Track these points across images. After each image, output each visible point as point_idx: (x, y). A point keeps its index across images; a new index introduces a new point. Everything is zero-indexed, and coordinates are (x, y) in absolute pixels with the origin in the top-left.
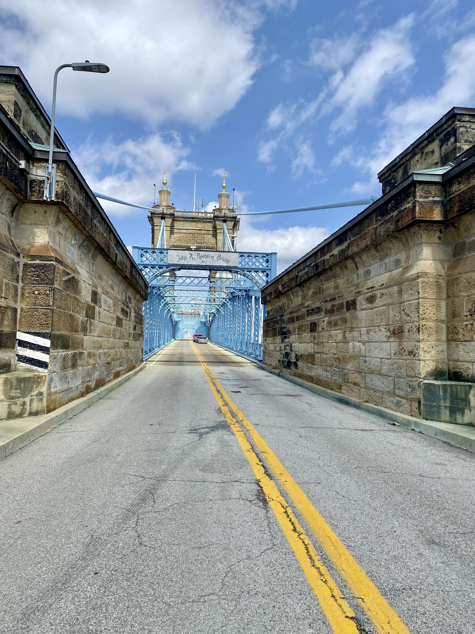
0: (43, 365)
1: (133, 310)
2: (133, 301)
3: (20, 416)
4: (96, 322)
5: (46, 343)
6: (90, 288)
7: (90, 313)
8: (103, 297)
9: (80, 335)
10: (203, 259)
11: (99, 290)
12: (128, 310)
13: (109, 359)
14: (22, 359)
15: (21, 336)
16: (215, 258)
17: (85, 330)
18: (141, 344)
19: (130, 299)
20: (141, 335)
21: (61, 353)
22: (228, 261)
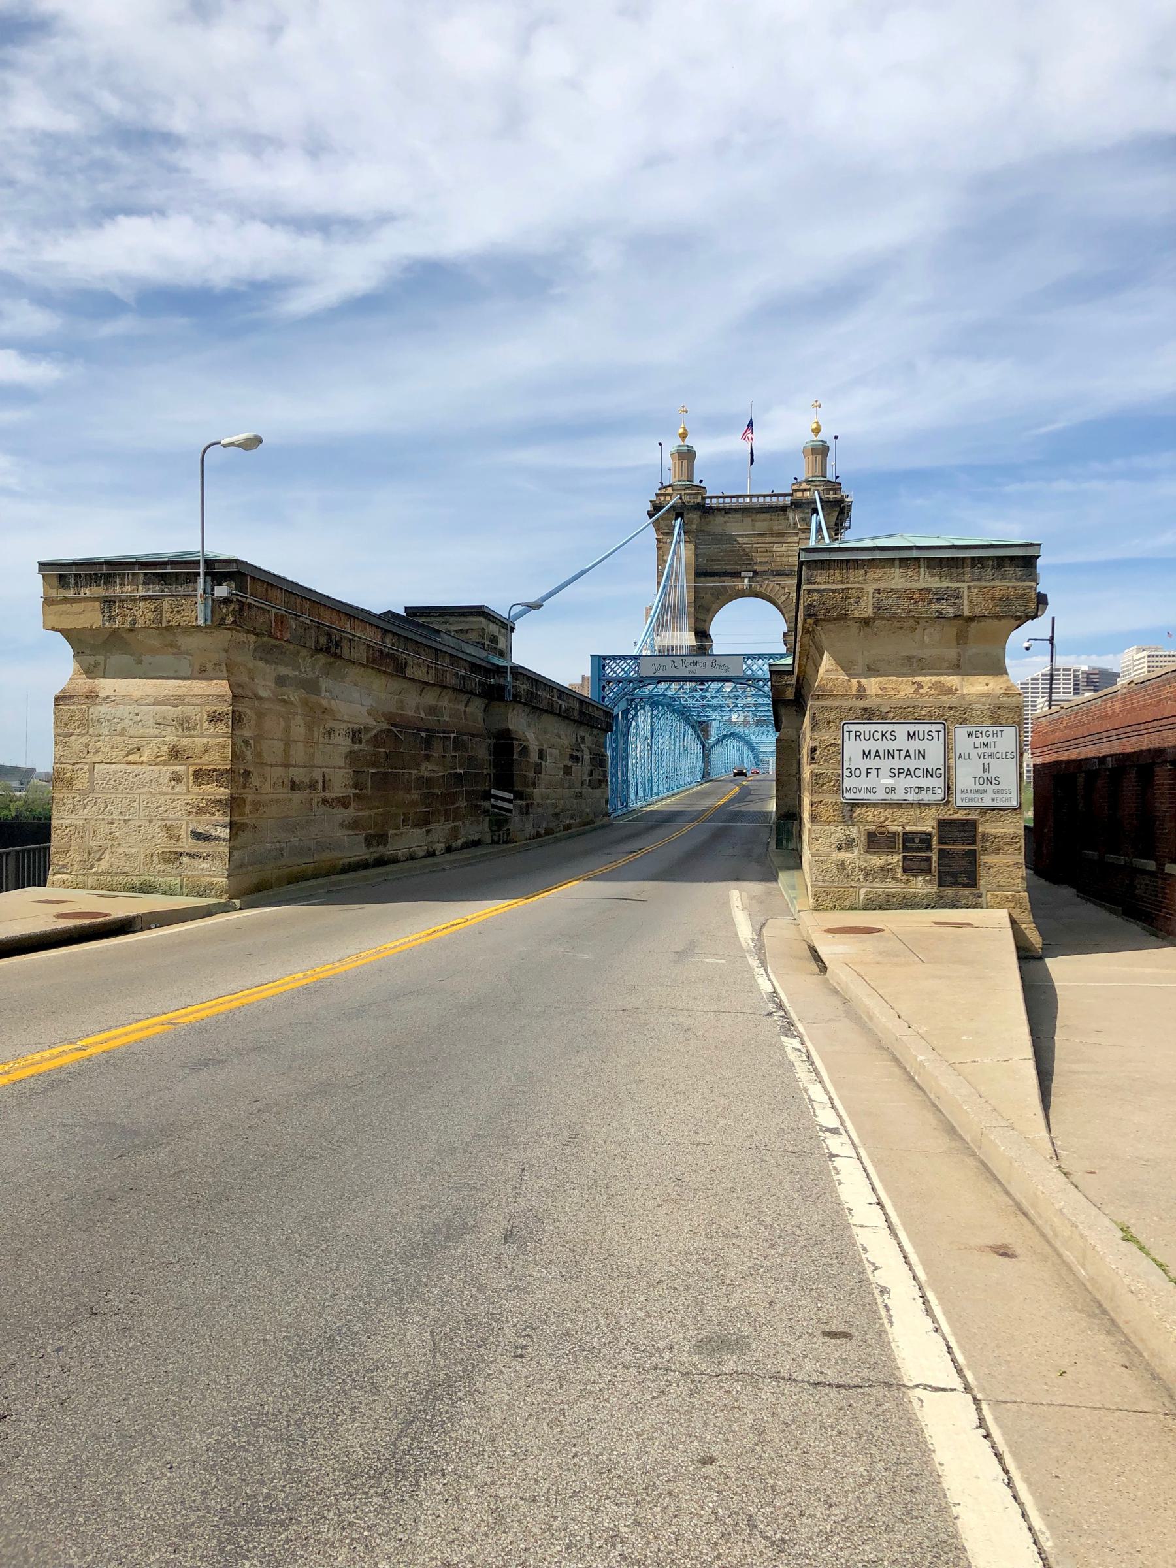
0: (510, 811)
1: (586, 752)
2: (589, 739)
3: (498, 843)
4: (542, 776)
5: (511, 796)
6: (537, 748)
7: (538, 769)
9: (530, 790)
10: (691, 668)
11: (545, 747)
12: (579, 754)
13: (557, 810)
14: (494, 806)
15: (494, 792)
16: (708, 665)
17: (534, 785)
18: (603, 793)
19: (583, 738)
20: (603, 781)
21: (519, 802)
22: (727, 669)
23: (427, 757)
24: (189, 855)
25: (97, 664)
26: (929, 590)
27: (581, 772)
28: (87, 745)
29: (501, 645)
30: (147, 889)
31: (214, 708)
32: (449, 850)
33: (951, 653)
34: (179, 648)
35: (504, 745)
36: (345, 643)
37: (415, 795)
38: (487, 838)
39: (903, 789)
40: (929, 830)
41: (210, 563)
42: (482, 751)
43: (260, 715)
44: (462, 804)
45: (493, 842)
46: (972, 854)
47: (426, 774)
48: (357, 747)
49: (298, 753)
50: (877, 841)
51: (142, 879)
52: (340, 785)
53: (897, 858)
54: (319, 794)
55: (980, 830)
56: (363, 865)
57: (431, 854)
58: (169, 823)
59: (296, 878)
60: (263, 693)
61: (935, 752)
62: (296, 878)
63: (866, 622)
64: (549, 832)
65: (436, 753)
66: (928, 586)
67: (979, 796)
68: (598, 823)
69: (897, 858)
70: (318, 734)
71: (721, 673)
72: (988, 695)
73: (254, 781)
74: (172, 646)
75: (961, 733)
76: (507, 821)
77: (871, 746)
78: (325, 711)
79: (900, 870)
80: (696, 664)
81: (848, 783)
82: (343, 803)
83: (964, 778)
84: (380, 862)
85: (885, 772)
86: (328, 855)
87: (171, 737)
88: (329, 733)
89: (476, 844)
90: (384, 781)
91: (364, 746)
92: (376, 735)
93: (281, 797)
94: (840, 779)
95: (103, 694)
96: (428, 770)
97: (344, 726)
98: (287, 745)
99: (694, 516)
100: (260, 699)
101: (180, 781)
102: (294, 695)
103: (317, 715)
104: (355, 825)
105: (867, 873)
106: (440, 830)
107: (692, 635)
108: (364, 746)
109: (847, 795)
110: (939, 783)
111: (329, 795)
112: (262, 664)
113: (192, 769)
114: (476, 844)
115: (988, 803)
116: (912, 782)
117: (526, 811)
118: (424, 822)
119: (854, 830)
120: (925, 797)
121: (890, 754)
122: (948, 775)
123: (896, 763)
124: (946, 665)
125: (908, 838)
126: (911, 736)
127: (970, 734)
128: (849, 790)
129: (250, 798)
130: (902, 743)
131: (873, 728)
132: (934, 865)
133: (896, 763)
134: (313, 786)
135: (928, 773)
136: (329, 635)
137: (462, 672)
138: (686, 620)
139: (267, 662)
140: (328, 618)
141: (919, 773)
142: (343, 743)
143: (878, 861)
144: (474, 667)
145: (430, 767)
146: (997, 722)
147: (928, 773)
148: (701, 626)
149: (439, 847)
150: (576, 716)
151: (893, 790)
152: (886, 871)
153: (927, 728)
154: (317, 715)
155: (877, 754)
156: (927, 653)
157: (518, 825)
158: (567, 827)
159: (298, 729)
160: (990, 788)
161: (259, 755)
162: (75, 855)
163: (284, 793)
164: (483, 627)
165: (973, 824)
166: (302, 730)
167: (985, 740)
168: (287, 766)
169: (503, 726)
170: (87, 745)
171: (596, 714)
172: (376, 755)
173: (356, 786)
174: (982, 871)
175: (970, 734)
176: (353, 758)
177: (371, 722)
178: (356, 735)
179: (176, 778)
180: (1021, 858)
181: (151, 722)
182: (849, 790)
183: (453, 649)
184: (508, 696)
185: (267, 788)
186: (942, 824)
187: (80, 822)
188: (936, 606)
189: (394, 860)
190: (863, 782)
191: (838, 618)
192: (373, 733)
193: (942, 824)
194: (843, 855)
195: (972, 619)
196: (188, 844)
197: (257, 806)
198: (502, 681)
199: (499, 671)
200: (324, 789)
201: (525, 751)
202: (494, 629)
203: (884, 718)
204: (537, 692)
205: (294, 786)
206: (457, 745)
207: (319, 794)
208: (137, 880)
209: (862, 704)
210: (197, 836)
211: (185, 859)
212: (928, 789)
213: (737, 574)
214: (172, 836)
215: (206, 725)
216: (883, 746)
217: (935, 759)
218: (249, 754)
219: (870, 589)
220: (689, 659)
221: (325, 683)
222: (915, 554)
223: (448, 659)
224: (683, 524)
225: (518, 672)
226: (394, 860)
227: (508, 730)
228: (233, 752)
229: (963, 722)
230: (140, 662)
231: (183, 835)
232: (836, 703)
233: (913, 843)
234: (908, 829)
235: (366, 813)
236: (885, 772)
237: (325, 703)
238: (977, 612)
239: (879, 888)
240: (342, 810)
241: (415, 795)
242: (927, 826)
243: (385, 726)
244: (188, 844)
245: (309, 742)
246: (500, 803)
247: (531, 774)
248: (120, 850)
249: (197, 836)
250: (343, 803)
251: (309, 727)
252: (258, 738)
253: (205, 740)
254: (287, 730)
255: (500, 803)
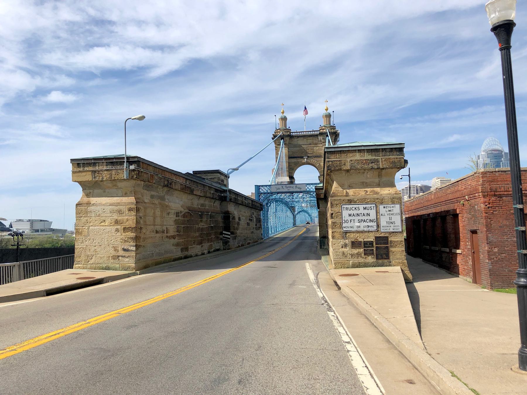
0: (229, 238)
1: (254, 218)
5: (229, 233)
7: (238, 224)
8: (242, 218)
9: (236, 231)
15: (224, 232)
16: (294, 187)
17: (237, 229)
20: (260, 227)
23: (201, 221)
24: (122, 256)
25: (90, 193)
26: (368, 160)
27: (253, 224)
28: (87, 220)
29: (225, 183)
30: (107, 268)
31: (129, 207)
32: (209, 252)
33: (377, 180)
34: (118, 186)
35: (227, 216)
36: (173, 184)
37: (197, 234)
38: (222, 248)
39: (363, 226)
40: (372, 240)
41: (128, 158)
42: (220, 218)
43: (145, 208)
44: (213, 236)
45: (224, 249)
46: (387, 248)
47: (201, 227)
48: (177, 218)
49: (158, 221)
50: (355, 244)
51: (106, 265)
52: (172, 231)
53: (362, 250)
54: (165, 235)
55: (390, 239)
56: (180, 258)
57: (203, 254)
58: (115, 246)
59: (157, 264)
60: (146, 201)
61: (373, 213)
62: (157, 264)
63: (348, 171)
64: (242, 245)
65: (204, 219)
66: (368, 158)
67: (388, 228)
68: (259, 242)
69: (362, 250)
70: (165, 214)
71: (299, 190)
72: (390, 194)
73: (144, 231)
74: (115, 186)
75: (381, 207)
76: (228, 242)
77: (351, 212)
78: (167, 206)
79: (363, 254)
80: (290, 187)
81: (344, 225)
82: (173, 237)
83: (383, 222)
84: (186, 257)
85: (356, 221)
86: (169, 255)
87: (116, 217)
88: (168, 214)
89: (218, 250)
90: (187, 229)
91: (180, 218)
92: (184, 214)
93: (152, 236)
94: (341, 224)
95: (92, 203)
96: (202, 225)
97: (173, 211)
98: (154, 218)
99: (287, 139)
100: (145, 203)
101: (119, 231)
102: (157, 202)
103: (164, 208)
104: (177, 245)
105: (352, 255)
106: (206, 245)
107: (288, 178)
108: (180, 218)
109: (344, 229)
110: (375, 224)
111: (168, 235)
112: (146, 191)
113: (122, 227)
114: (218, 250)
115: (392, 230)
116: (366, 224)
117: (235, 238)
118: (200, 243)
119: (347, 241)
120: (370, 229)
121: (358, 215)
122: (378, 221)
123: (360, 218)
124: (375, 184)
125: (365, 243)
126: (365, 208)
127: (384, 207)
128: (345, 227)
129: (142, 236)
130: (362, 211)
131: (351, 206)
132: (375, 252)
133: (360, 218)
134: (163, 232)
135: (371, 221)
136: (168, 181)
137: (212, 192)
138: (286, 173)
139: (147, 190)
140: (168, 175)
141: (368, 221)
142: (173, 217)
143: (355, 251)
144: (217, 190)
145: (202, 224)
146: (393, 203)
147: (371, 221)
148: (291, 175)
149: (206, 252)
150: (250, 205)
151: (359, 227)
152: (359, 254)
153: (370, 206)
154: (164, 208)
155: (354, 215)
156: (368, 181)
157: (232, 243)
158: (249, 243)
159: (158, 213)
160: (392, 225)
161: (145, 222)
162: (83, 258)
163: (153, 235)
164: (219, 176)
165: (387, 238)
166: (159, 213)
167: (390, 209)
168: (155, 225)
169: (226, 210)
170: (87, 220)
171: (258, 205)
172: (184, 221)
173: (177, 232)
174: (391, 254)
175: (384, 207)
176: (176, 222)
177: (182, 210)
178: (177, 214)
179: (117, 230)
180: (404, 249)
181: (109, 212)
182: (345, 227)
183: (209, 184)
184: (228, 199)
185: (148, 233)
186: (376, 238)
187: (84, 246)
188: (371, 165)
189: (191, 256)
190: (349, 225)
191: (338, 170)
192: (183, 213)
193: (376, 238)
194: (343, 249)
195: (383, 169)
196: (121, 253)
197: (144, 239)
198: (226, 195)
199: (225, 191)
200: (167, 233)
201: (234, 218)
202: (222, 177)
203: (355, 202)
204: (238, 198)
205: (157, 232)
206: (211, 217)
207: (165, 235)
208: (104, 266)
209: (348, 198)
210: (124, 250)
211: (120, 258)
212: (371, 226)
213: (302, 157)
214: (116, 250)
215: (127, 212)
216: (355, 212)
217: (373, 216)
218: (142, 221)
219: (349, 160)
220: (288, 186)
221: (167, 197)
222: (363, 148)
223: (207, 187)
224: (284, 141)
225: (231, 191)
226: (191, 256)
227: (228, 211)
228: (136, 221)
229: (382, 203)
230: (105, 192)
231: (119, 249)
232: (339, 198)
233: (367, 245)
234: (365, 240)
235: (182, 240)
236: (356, 221)
237: (167, 203)
238: (385, 166)
239: (356, 260)
240: (173, 240)
241: (197, 234)
242: (372, 239)
243: (187, 211)
244: (121, 253)
245: (162, 217)
246: (226, 236)
247: (236, 226)
248: (98, 256)
249: (124, 250)
250: (173, 237)
251: (162, 212)
252: (145, 216)
253: (127, 217)
254: (154, 213)
255: (226, 236)
